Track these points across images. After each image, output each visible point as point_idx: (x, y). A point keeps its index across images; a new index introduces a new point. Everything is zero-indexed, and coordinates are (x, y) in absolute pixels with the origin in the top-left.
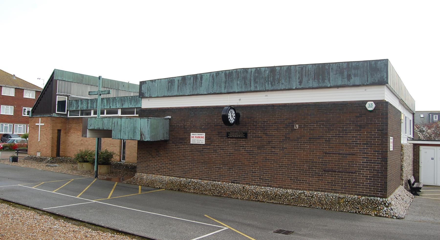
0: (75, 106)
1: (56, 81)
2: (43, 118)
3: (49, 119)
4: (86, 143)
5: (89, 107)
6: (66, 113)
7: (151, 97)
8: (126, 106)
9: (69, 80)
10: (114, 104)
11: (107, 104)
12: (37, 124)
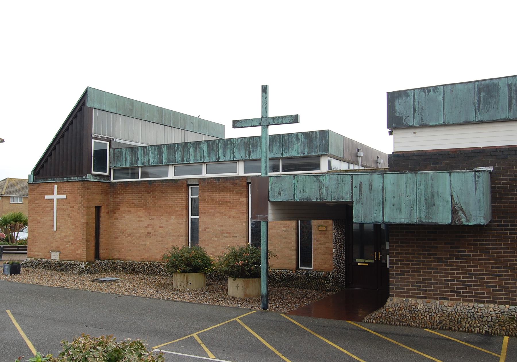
0: (129, 159)
1: (91, 109)
2: (61, 185)
3: (79, 185)
4: (161, 231)
5: (164, 160)
6: (107, 173)
7: (423, 126)
9: (112, 111)
10: (228, 152)
11: (210, 154)
12: (47, 197)
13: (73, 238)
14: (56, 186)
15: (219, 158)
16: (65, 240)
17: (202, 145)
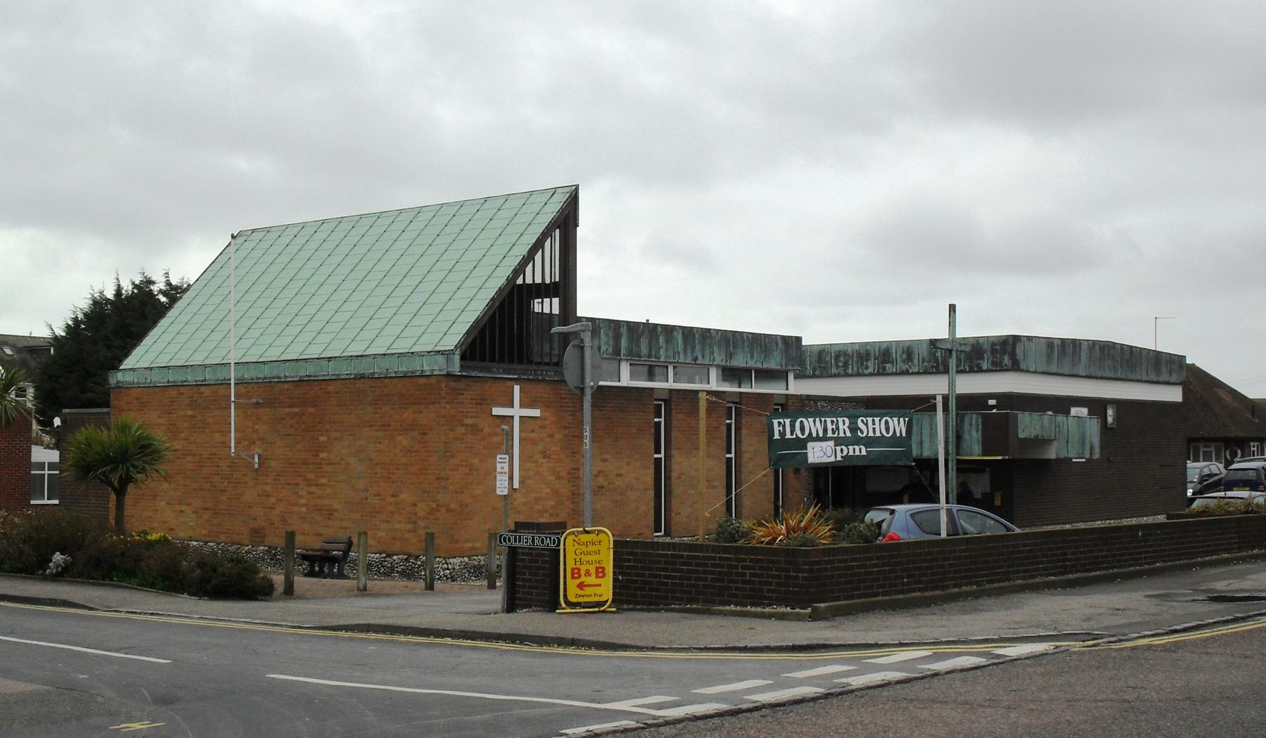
4: (619, 482)
5: (623, 351)
8: (739, 361)
10: (707, 351)
12: (497, 411)
13: (552, 503)
14: (517, 388)
15: (696, 359)
16: (537, 507)
17: (675, 333)
